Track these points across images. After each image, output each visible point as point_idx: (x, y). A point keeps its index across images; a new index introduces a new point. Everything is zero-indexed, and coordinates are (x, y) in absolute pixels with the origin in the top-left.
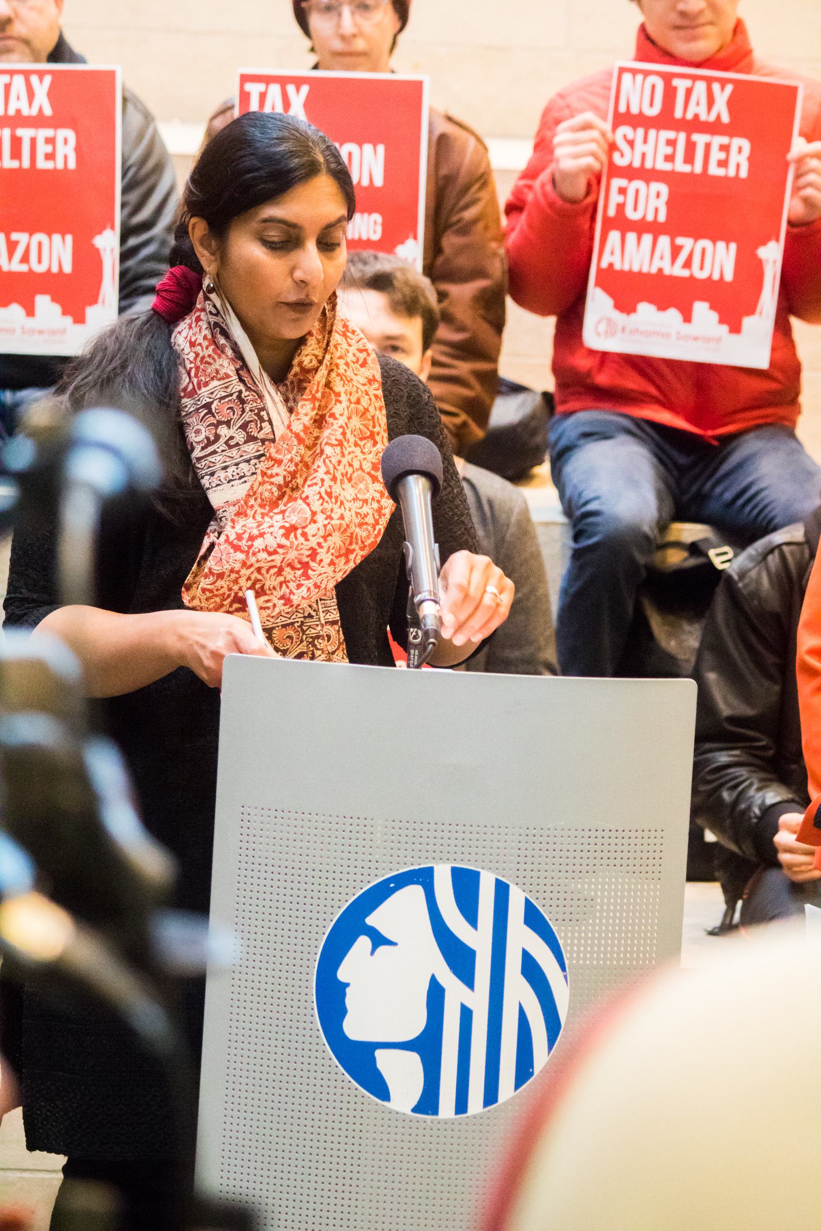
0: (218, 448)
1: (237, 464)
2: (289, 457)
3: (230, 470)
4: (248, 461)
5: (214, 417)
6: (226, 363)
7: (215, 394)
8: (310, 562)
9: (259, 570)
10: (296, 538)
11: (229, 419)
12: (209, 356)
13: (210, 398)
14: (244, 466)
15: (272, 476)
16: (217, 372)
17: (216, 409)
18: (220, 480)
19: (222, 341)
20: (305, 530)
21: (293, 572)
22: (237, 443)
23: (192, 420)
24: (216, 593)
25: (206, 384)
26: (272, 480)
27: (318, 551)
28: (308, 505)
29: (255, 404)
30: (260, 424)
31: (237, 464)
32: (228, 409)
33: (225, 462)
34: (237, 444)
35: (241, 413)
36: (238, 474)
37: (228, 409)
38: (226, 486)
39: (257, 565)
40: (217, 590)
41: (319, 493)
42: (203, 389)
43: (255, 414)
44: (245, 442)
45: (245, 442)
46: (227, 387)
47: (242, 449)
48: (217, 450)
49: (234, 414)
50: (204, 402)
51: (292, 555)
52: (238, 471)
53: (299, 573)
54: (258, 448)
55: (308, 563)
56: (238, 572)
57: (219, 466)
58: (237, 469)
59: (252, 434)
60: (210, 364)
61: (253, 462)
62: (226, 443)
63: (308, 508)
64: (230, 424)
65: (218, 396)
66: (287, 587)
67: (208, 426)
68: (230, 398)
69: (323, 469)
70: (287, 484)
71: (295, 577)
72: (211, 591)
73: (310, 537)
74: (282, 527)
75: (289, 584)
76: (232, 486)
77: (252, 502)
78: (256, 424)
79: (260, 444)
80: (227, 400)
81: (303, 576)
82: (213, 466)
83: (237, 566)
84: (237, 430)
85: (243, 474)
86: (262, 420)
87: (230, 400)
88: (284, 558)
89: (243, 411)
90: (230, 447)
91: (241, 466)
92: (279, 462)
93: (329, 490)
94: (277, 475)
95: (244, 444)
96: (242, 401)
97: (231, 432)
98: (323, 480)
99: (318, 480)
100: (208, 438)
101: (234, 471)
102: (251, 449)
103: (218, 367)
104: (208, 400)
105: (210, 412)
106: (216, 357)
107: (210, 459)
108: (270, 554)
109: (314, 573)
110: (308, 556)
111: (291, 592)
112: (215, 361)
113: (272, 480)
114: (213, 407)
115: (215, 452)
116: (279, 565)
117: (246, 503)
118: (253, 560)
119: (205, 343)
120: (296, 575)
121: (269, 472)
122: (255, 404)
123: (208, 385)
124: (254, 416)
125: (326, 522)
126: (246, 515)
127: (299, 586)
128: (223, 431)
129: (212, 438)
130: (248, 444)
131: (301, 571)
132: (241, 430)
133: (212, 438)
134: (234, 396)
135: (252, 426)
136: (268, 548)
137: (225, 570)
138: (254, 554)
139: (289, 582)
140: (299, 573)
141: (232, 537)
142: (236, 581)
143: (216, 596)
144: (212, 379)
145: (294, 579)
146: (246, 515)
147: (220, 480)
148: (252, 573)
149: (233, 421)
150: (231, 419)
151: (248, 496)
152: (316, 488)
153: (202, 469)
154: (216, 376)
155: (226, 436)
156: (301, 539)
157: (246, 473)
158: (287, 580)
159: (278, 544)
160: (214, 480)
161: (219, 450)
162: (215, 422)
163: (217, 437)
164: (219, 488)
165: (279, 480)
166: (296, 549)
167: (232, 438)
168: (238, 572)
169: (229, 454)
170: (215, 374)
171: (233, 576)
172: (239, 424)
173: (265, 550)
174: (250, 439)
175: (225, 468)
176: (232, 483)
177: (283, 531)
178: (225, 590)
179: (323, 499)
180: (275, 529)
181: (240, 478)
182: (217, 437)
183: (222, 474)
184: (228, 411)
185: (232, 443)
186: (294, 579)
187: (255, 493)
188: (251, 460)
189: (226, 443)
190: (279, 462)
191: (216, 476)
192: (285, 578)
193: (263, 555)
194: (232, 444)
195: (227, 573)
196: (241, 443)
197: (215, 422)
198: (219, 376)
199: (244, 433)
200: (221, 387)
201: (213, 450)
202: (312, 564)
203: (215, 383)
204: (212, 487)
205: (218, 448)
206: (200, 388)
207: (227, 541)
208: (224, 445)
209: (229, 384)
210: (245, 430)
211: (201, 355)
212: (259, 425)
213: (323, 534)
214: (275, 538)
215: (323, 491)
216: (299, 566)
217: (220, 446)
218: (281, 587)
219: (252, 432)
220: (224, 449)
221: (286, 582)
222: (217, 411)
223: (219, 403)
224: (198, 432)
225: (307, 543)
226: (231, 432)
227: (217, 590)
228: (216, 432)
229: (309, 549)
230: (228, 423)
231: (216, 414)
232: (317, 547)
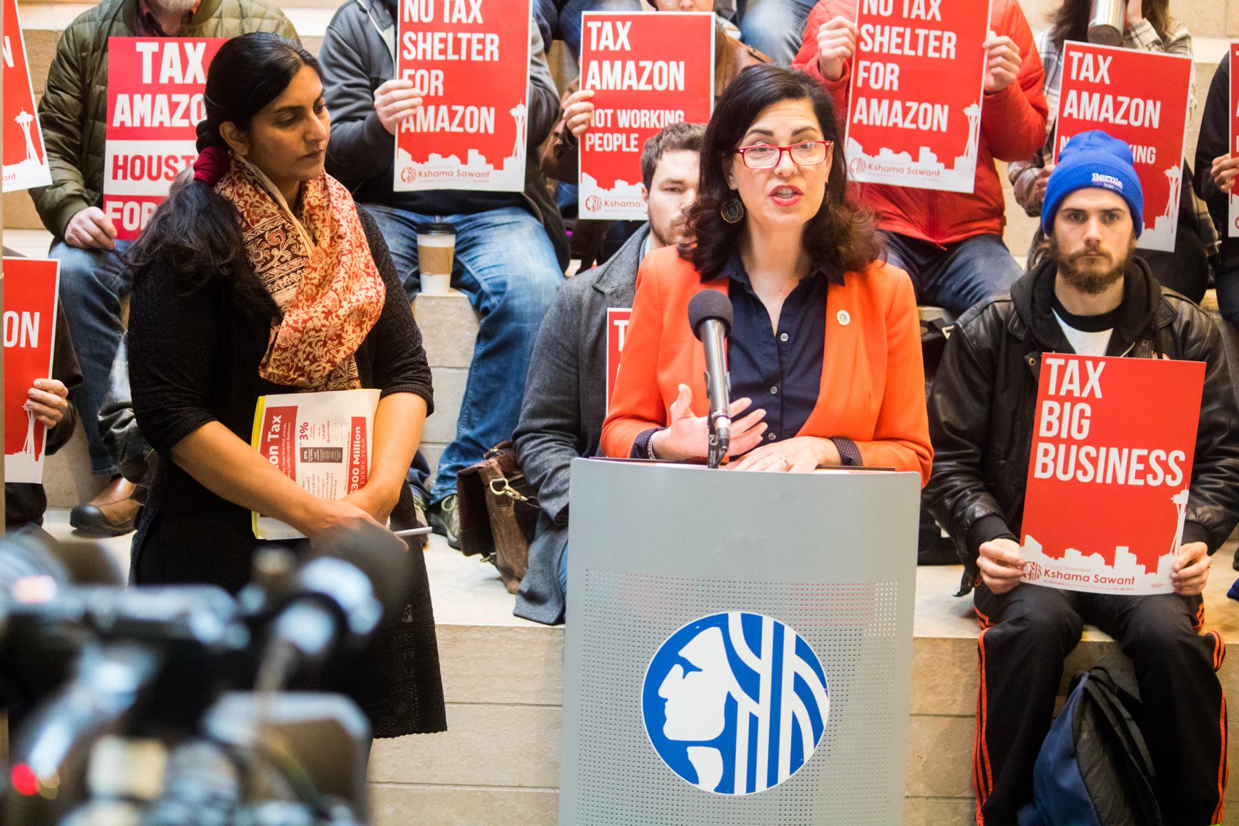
1: (288, 274)
2: (321, 266)
4: (295, 272)
6: (270, 205)
9: (310, 344)
12: (257, 202)
15: (311, 279)
16: (265, 212)
19: (262, 192)
20: (338, 313)
23: (252, 248)
25: (258, 221)
26: (312, 281)
28: (338, 295)
31: (288, 274)
34: (286, 261)
38: (284, 290)
39: (309, 341)
42: (256, 225)
44: (291, 259)
45: (291, 259)
50: (258, 234)
51: (331, 332)
53: (336, 342)
55: (340, 335)
56: (297, 346)
57: (277, 276)
60: (258, 207)
61: (298, 272)
62: (279, 260)
66: (330, 354)
69: (343, 271)
70: (320, 284)
72: (279, 360)
74: (323, 312)
77: (301, 298)
83: (296, 342)
86: (300, 244)
89: (287, 238)
90: (282, 263)
92: (315, 270)
94: (315, 278)
96: (285, 231)
97: (281, 253)
98: (344, 278)
99: (341, 278)
102: (295, 262)
104: (261, 232)
105: (264, 240)
106: (263, 202)
107: (269, 272)
108: (317, 331)
111: (334, 357)
112: (262, 204)
113: (312, 281)
114: (266, 236)
115: (272, 267)
117: (297, 298)
119: (252, 194)
121: (310, 276)
126: (298, 307)
127: (338, 352)
128: (275, 252)
129: (269, 258)
133: (269, 258)
134: (280, 228)
138: (307, 333)
140: (336, 342)
141: (291, 323)
142: (296, 354)
143: (283, 365)
144: (262, 217)
146: (298, 307)
151: (298, 293)
152: (341, 283)
153: (265, 280)
163: (272, 257)
165: (316, 282)
167: (282, 257)
168: (297, 346)
171: (294, 349)
173: (314, 329)
174: (294, 256)
175: (281, 278)
177: (323, 315)
178: (288, 361)
180: (319, 314)
181: (293, 284)
182: (272, 257)
183: (280, 282)
185: (283, 260)
187: (302, 292)
189: (279, 260)
190: (315, 270)
193: (312, 333)
203: (264, 220)
206: (253, 225)
207: (287, 325)
210: (290, 251)
211: (250, 201)
217: (275, 263)
221: (328, 351)
224: (258, 254)
226: (281, 253)
227: (284, 360)
230: (278, 247)
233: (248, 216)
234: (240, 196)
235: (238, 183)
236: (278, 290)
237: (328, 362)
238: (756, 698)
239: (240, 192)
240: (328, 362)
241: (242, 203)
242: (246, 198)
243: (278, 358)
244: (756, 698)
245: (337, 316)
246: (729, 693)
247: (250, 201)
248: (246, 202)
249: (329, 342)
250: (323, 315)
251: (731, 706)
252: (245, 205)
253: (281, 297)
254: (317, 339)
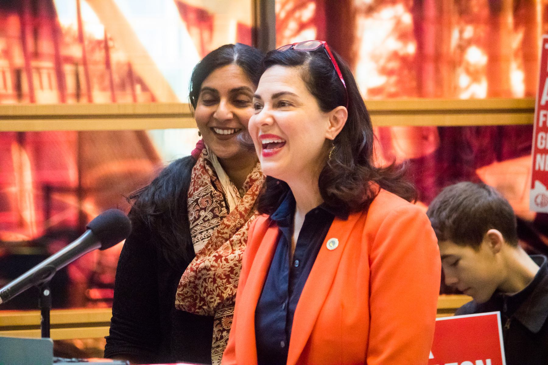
0: (199, 222)
1: (207, 230)
3: (203, 234)
4: (213, 228)
5: (199, 206)
7: (200, 194)
8: (230, 274)
10: (221, 262)
11: (206, 206)
13: (198, 196)
14: (211, 231)
16: (202, 182)
17: (200, 202)
18: (198, 239)
21: (221, 281)
22: (209, 219)
24: (186, 296)
27: (234, 268)
29: (218, 198)
30: (221, 209)
31: (207, 230)
32: (205, 202)
33: (202, 229)
34: (208, 220)
35: (211, 203)
36: (207, 235)
37: (205, 202)
39: (204, 277)
40: (186, 294)
41: (240, 240)
43: (218, 203)
44: (213, 218)
45: (213, 218)
46: (206, 190)
47: (210, 222)
48: (198, 223)
49: (208, 204)
52: (207, 234)
53: (225, 281)
54: (218, 221)
55: (229, 275)
56: (194, 282)
57: (198, 231)
58: (207, 233)
59: (216, 214)
60: (200, 178)
62: (203, 219)
63: (231, 247)
64: (206, 210)
65: (202, 195)
67: (196, 211)
68: (207, 196)
71: (223, 283)
73: (229, 261)
75: (220, 288)
76: (204, 242)
77: (210, 247)
78: (219, 209)
79: (220, 219)
80: (205, 197)
81: (227, 282)
82: (196, 232)
83: (192, 279)
84: (209, 212)
85: (209, 235)
87: (207, 197)
88: (215, 273)
89: (213, 202)
90: (205, 221)
91: (209, 231)
93: (246, 239)
95: (211, 219)
96: (212, 197)
100: (195, 217)
101: (205, 234)
102: (215, 221)
105: (197, 204)
109: (233, 280)
110: (229, 271)
112: (202, 176)
114: (199, 201)
115: (197, 225)
116: (213, 277)
118: (200, 274)
120: (223, 282)
122: (218, 198)
123: (198, 190)
124: (217, 204)
125: (240, 253)
128: (203, 213)
130: (213, 219)
131: (226, 280)
132: (211, 212)
133: (197, 217)
134: (209, 195)
135: (216, 210)
136: (207, 267)
137: (186, 282)
139: (220, 286)
140: (225, 281)
145: (222, 285)
147: (198, 239)
148: (203, 282)
149: (207, 208)
150: (207, 207)
152: (239, 237)
155: (203, 216)
156: (224, 262)
157: (211, 235)
158: (219, 285)
159: (211, 265)
160: (196, 239)
161: (199, 223)
162: (199, 209)
163: (199, 216)
164: (197, 243)
166: (221, 268)
167: (206, 216)
169: (204, 225)
170: (201, 184)
171: (192, 285)
172: (210, 209)
174: (215, 216)
175: (201, 233)
176: (204, 240)
177: (214, 258)
179: (242, 244)
182: (199, 216)
183: (199, 236)
184: (206, 202)
185: (206, 219)
186: (222, 285)
188: (214, 227)
189: (203, 219)
191: (196, 237)
192: (218, 285)
193: (204, 272)
194: (206, 220)
195: (188, 284)
196: (210, 219)
197: (199, 209)
198: (203, 185)
199: (212, 213)
200: (203, 190)
201: (196, 223)
202: (231, 275)
204: (195, 243)
205: (199, 222)
208: (202, 221)
209: (207, 188)
212: (220, 209)
213: (238, 259)
214: (210, 262)
215: (242, 239)
216: (224, 277)
217: (200, 221)
218: (216, 290)
219: (216, 213)
220: (201, 222)
221: (218, 287)
222: (201, 203)
223: (202, 199)
225: (227, 264)
228: (199, 214)
229: (229, 268)
230: (205, 209)
231: (200, 205)
232: (234, 266)
236: (197, 242)
237: (218, 295)
240: (218, 295)
243: (181, 292)
245: (226, 260)
249: (218, 280)
250: (214, 258)
253: (198, 247)
254: (208, 276)
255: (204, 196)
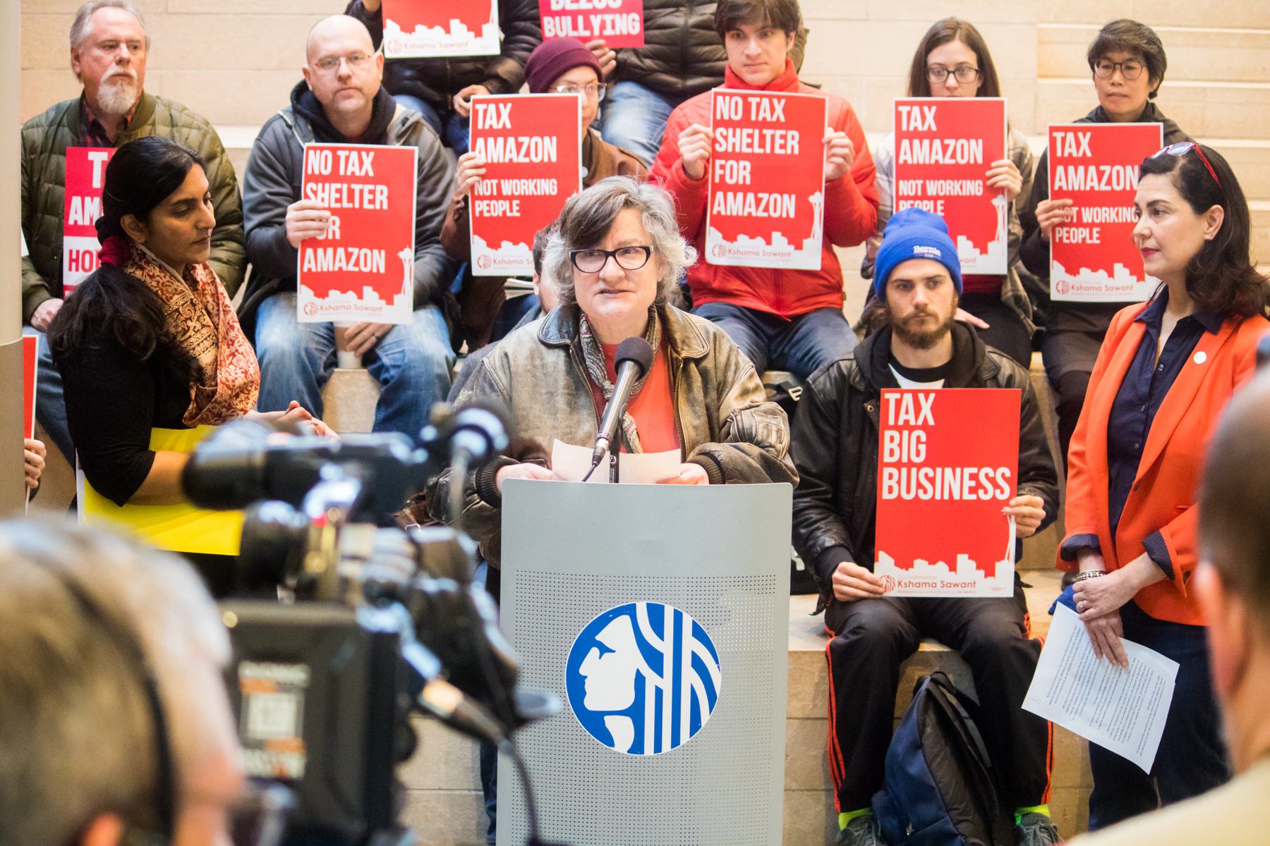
12: (168, 281)
16: (176, 290)
25: (171, 298)
42: (172, 301)
57: (196, 344)
60: (169, 286)
90: (196, 332)
103: (175, 286)
105: (180, 313)
107: (189, 340)
119: (162, 275)
128: (189, 323)
144: (174, 294)
154: (176, 292)
167: (195, 327)
175: (199, 345)
182: (189, 327)
203: (176, 297)
211: (161, 281)
217: (191, 333)
230: (190, 319)
233: (163, 294)
234: (152, 277)
235: (146, 266)
238: (659, 671)
239: (151, 274)
241: (154, 284)
242: (158, 278)
244: (659, 671)
246: (638, 671)
247: (161, 281)
248: (158, 282)
251: (640, 681)
252: (158, 284)
255: (183, 305)
